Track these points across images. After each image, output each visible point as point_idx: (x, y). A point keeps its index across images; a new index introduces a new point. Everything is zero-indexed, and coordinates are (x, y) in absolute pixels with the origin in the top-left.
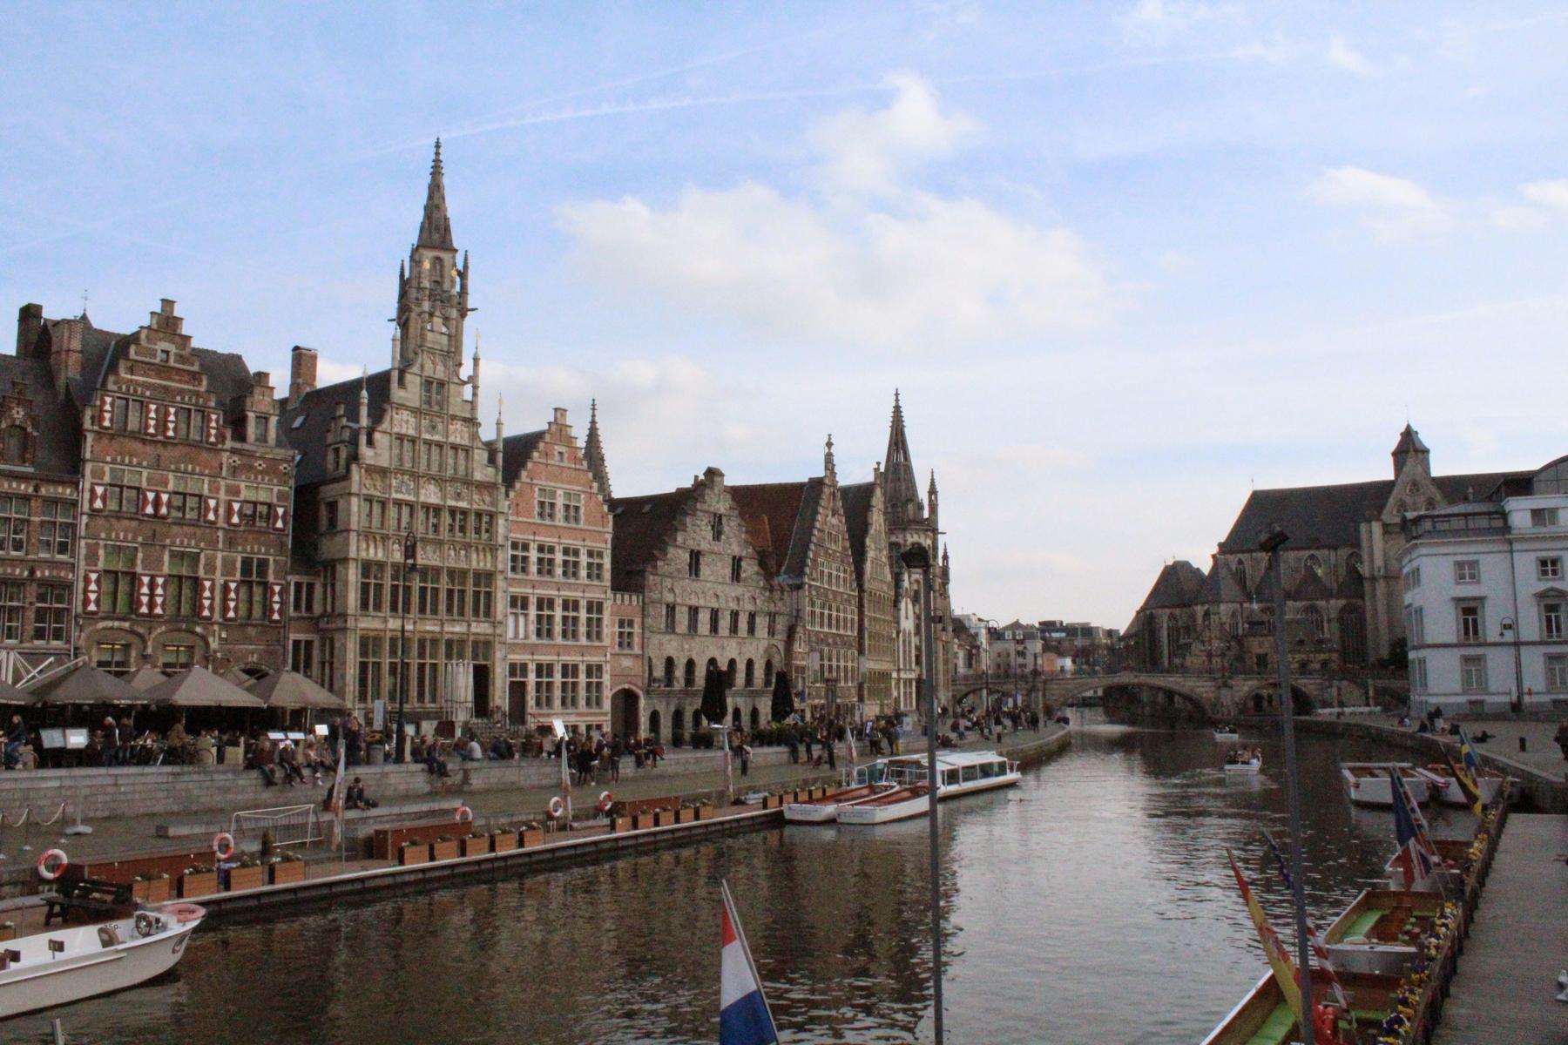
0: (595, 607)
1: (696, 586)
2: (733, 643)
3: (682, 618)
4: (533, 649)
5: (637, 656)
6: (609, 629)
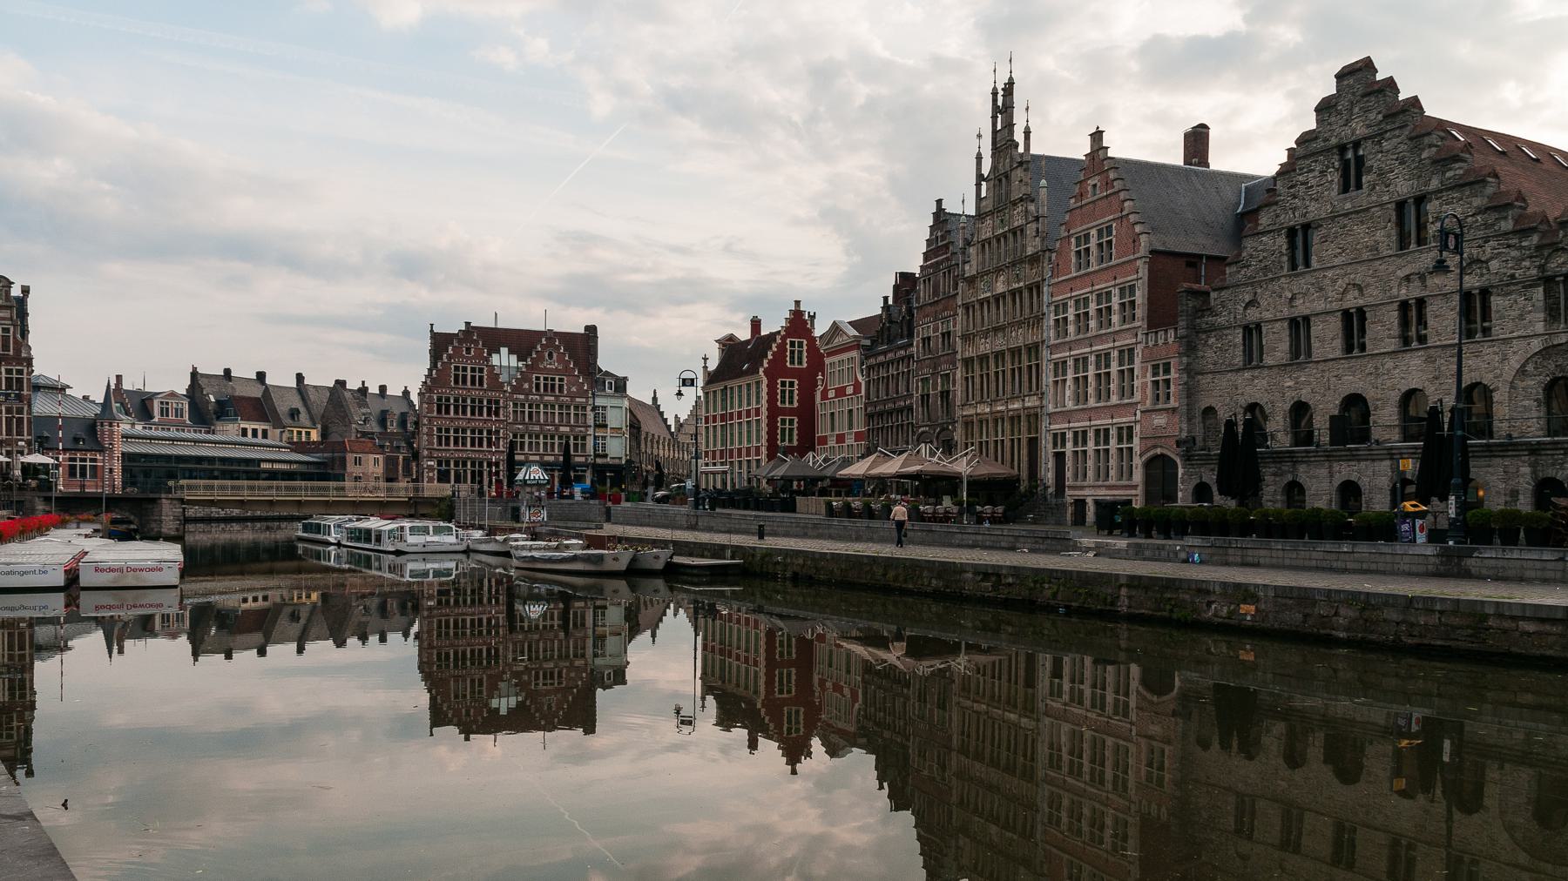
0: (1127, 354)
1: (1303, 283)
2: (1415, 361)
3: (1278, 344)
4: (1068, 415)
5: (1174, 410)
6: (1143, 379)
